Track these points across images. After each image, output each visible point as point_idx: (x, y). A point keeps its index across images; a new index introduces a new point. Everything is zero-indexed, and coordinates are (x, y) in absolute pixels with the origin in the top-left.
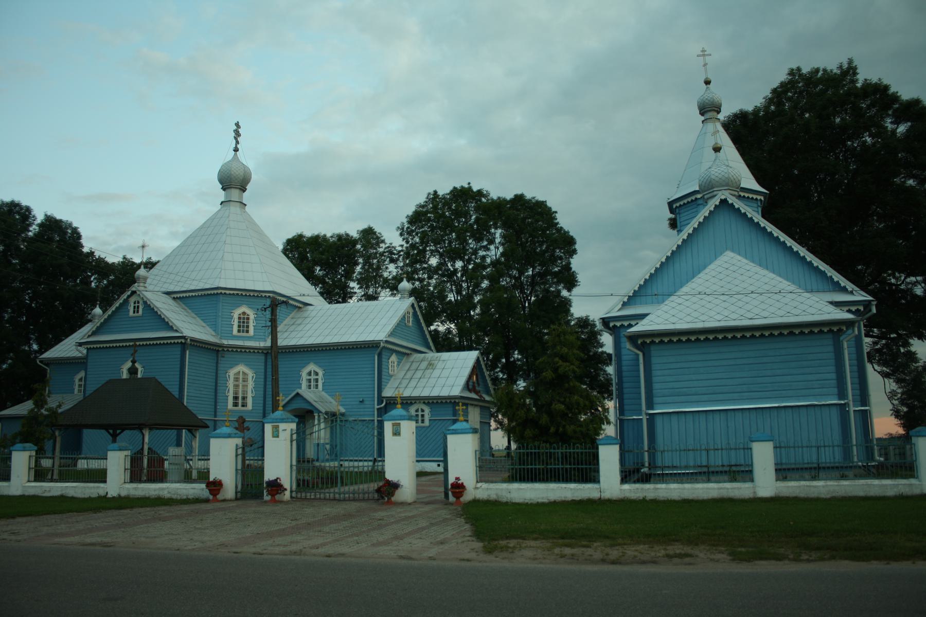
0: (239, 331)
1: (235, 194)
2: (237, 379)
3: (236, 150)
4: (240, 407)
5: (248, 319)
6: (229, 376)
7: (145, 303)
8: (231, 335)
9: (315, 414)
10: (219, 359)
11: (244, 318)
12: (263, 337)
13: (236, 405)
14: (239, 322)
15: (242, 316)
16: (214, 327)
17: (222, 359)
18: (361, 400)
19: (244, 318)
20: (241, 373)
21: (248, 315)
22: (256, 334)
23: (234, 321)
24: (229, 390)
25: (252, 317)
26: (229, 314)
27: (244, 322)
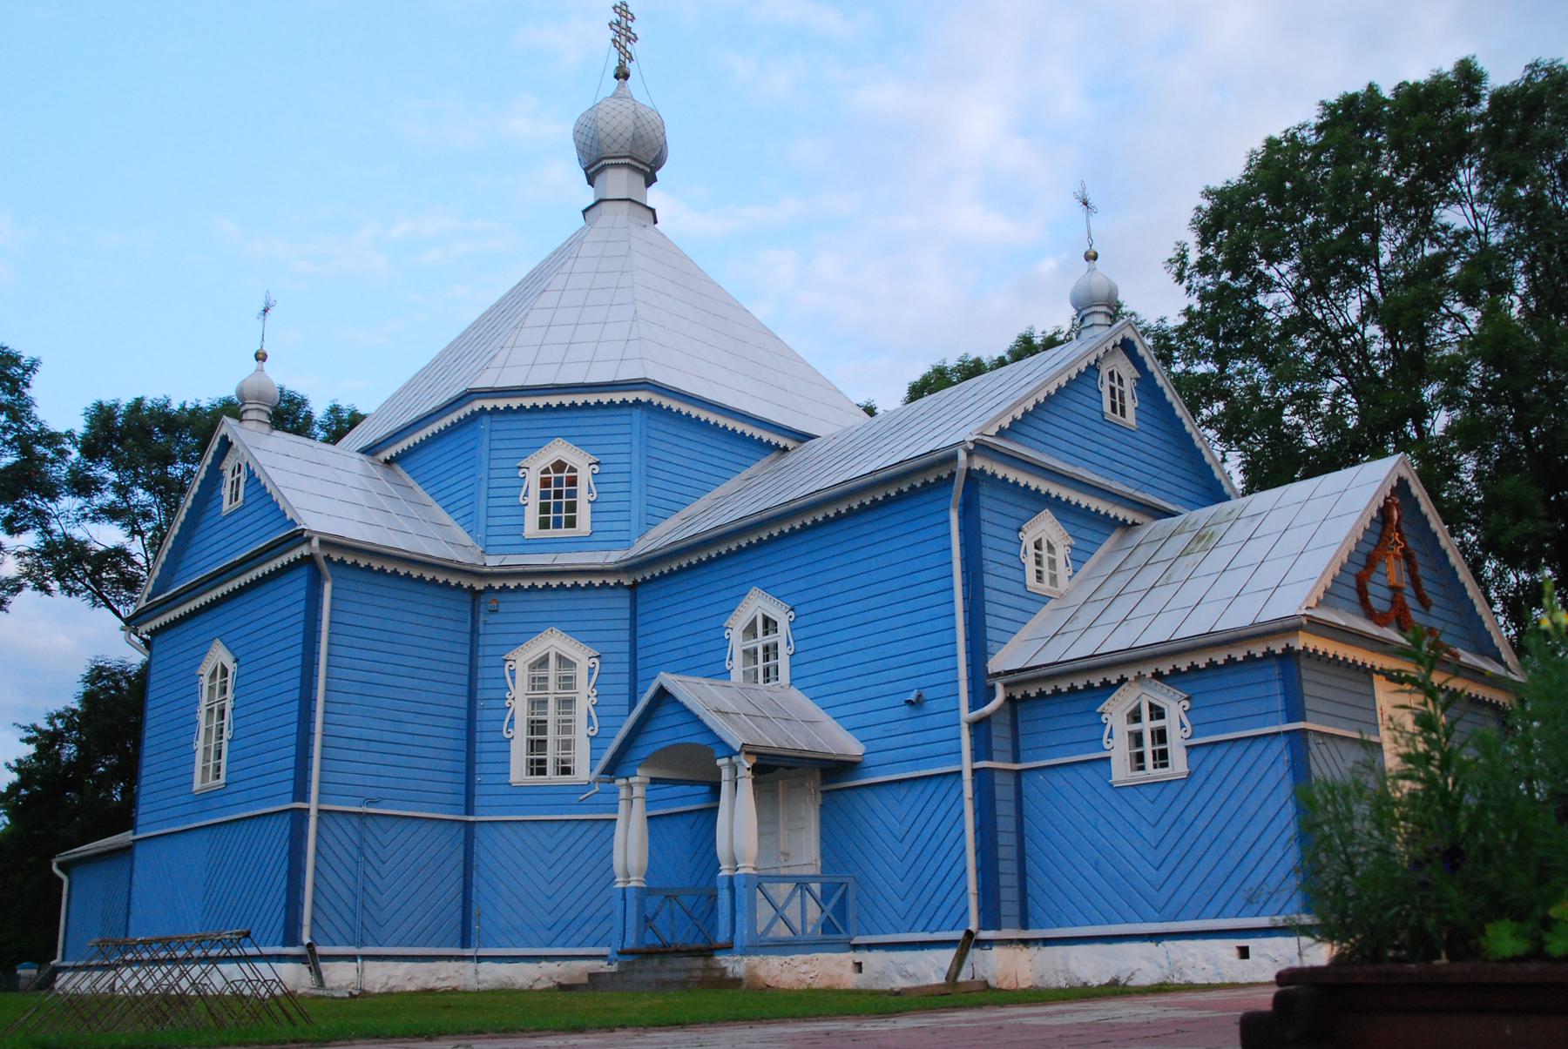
0: (544, 524)
1: (618, 182)
2: (539, 683)
3: (622, 75)
4: (552, 777)
5: (572, 482)
6: (513, 672)
7: (251, 474)
8: (517, 540)
9: (719, 762)
10: (482, 618)
11: (559, 482)
12: (624, 536)
13: (538, 767)
14: (544, 495)
15: (553, 475)
16: (468, 520)
17: (492, 618)
18: (913, 696)
19: (559, 482)
20: (552, 661)
21: (572, 470)
22: (598, 526)
23: (526, 495)
24: (512, 720)
25: (584, 476)
26: (510, 473)
27: (559, 486)
